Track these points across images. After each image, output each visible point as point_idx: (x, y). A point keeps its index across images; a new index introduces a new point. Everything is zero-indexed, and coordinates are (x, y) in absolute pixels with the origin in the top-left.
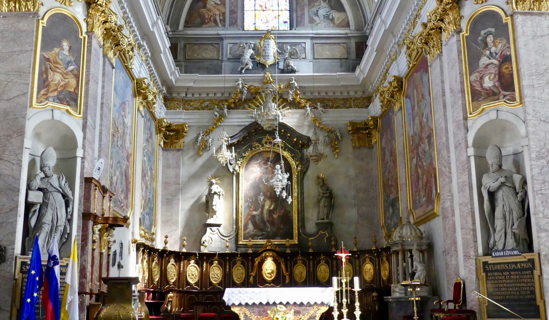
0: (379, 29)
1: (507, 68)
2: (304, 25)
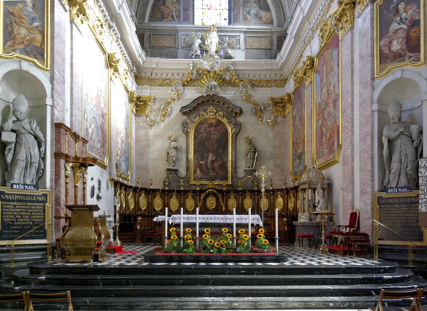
2: (239, 22)
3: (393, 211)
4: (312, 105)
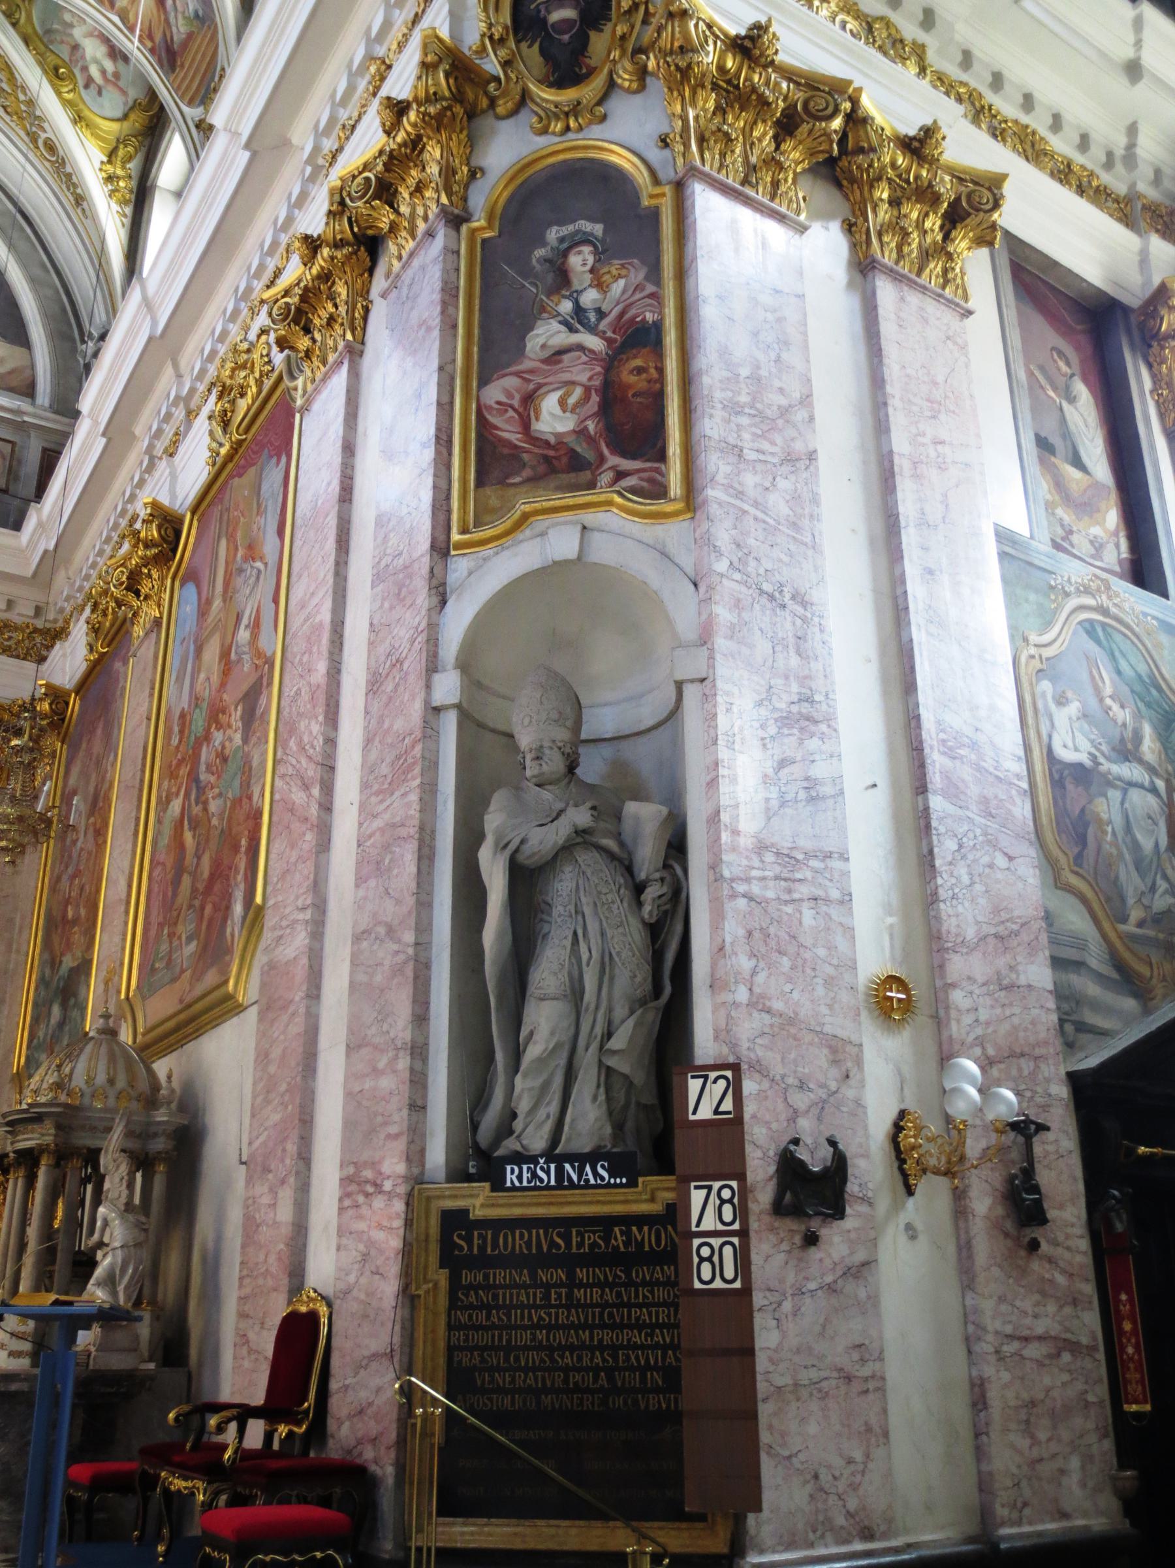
0: (131, 332)
1: (639, 370)
3: (530, 1307)
4: (148, 727)
